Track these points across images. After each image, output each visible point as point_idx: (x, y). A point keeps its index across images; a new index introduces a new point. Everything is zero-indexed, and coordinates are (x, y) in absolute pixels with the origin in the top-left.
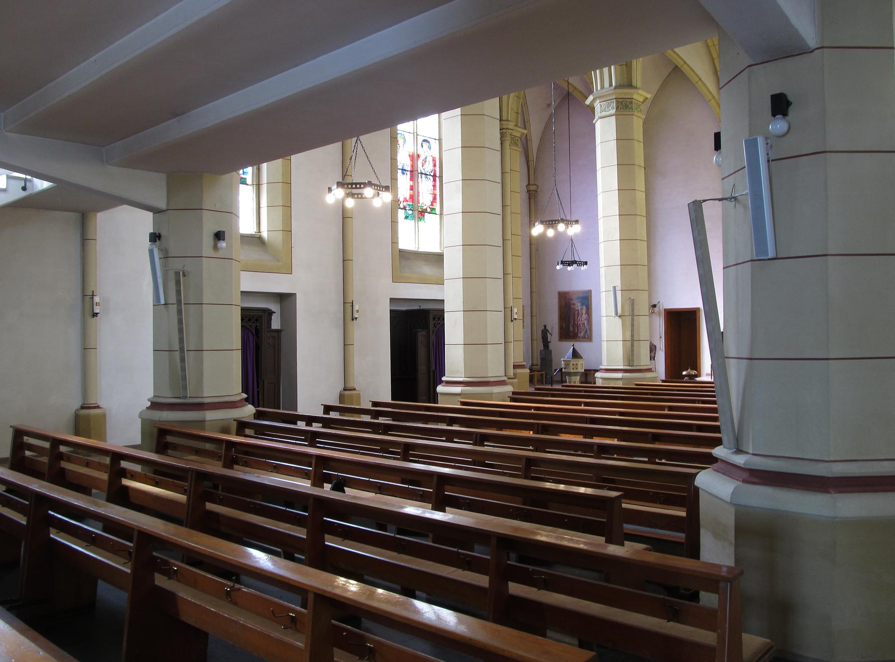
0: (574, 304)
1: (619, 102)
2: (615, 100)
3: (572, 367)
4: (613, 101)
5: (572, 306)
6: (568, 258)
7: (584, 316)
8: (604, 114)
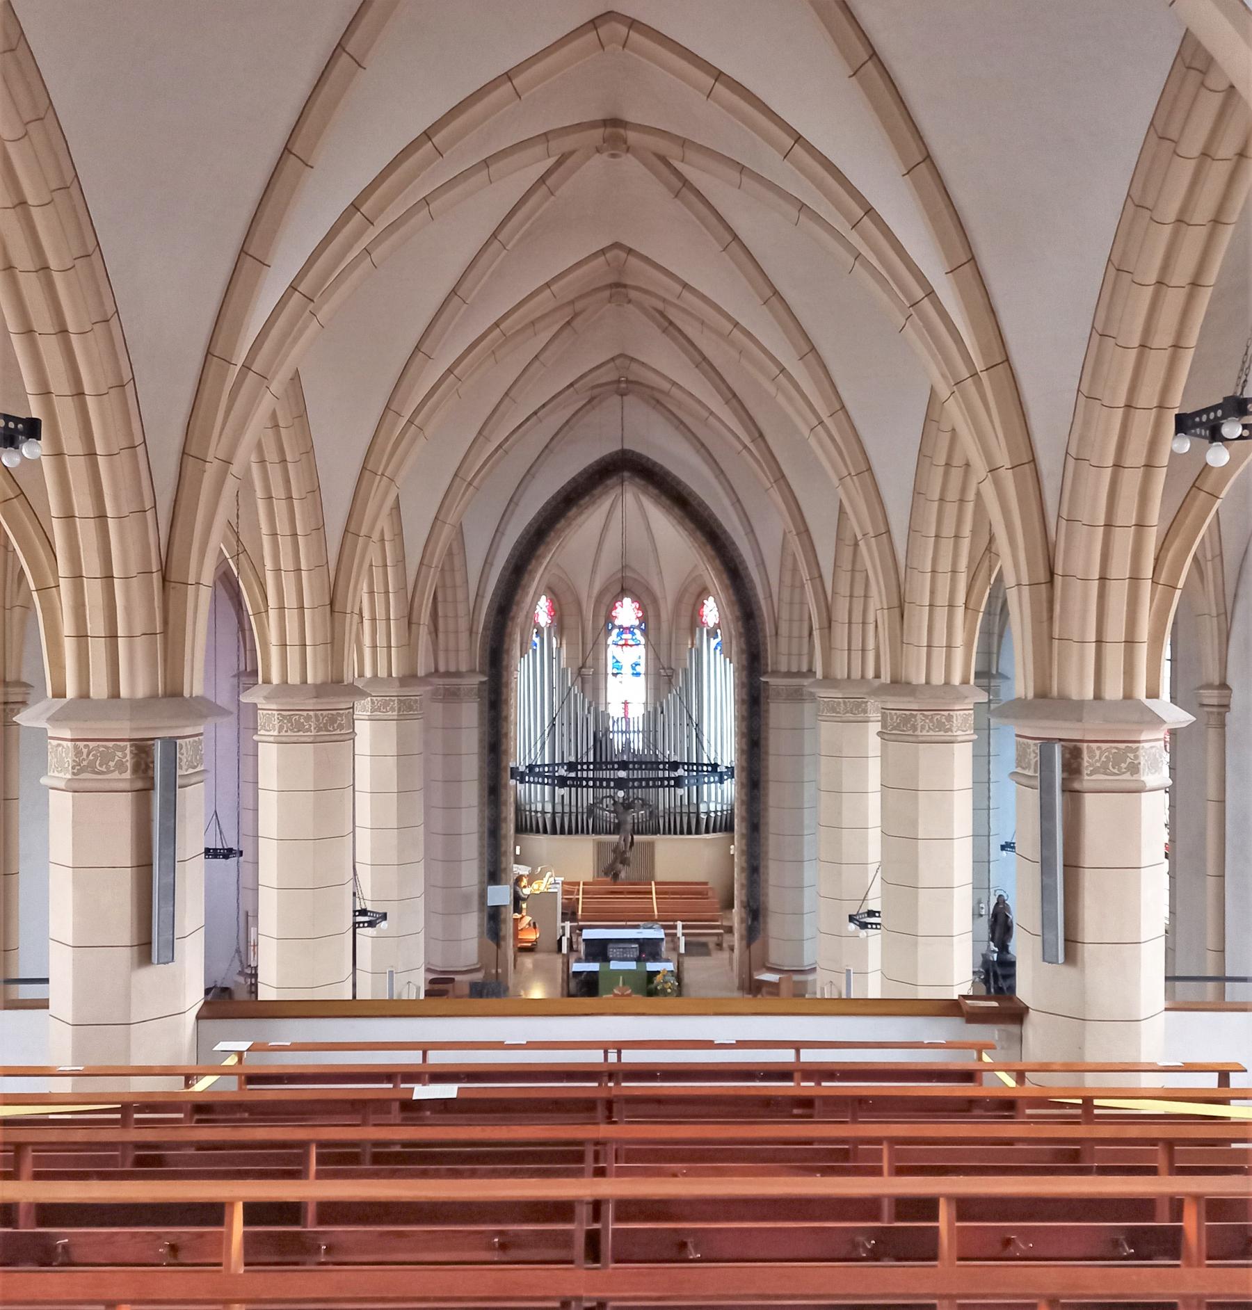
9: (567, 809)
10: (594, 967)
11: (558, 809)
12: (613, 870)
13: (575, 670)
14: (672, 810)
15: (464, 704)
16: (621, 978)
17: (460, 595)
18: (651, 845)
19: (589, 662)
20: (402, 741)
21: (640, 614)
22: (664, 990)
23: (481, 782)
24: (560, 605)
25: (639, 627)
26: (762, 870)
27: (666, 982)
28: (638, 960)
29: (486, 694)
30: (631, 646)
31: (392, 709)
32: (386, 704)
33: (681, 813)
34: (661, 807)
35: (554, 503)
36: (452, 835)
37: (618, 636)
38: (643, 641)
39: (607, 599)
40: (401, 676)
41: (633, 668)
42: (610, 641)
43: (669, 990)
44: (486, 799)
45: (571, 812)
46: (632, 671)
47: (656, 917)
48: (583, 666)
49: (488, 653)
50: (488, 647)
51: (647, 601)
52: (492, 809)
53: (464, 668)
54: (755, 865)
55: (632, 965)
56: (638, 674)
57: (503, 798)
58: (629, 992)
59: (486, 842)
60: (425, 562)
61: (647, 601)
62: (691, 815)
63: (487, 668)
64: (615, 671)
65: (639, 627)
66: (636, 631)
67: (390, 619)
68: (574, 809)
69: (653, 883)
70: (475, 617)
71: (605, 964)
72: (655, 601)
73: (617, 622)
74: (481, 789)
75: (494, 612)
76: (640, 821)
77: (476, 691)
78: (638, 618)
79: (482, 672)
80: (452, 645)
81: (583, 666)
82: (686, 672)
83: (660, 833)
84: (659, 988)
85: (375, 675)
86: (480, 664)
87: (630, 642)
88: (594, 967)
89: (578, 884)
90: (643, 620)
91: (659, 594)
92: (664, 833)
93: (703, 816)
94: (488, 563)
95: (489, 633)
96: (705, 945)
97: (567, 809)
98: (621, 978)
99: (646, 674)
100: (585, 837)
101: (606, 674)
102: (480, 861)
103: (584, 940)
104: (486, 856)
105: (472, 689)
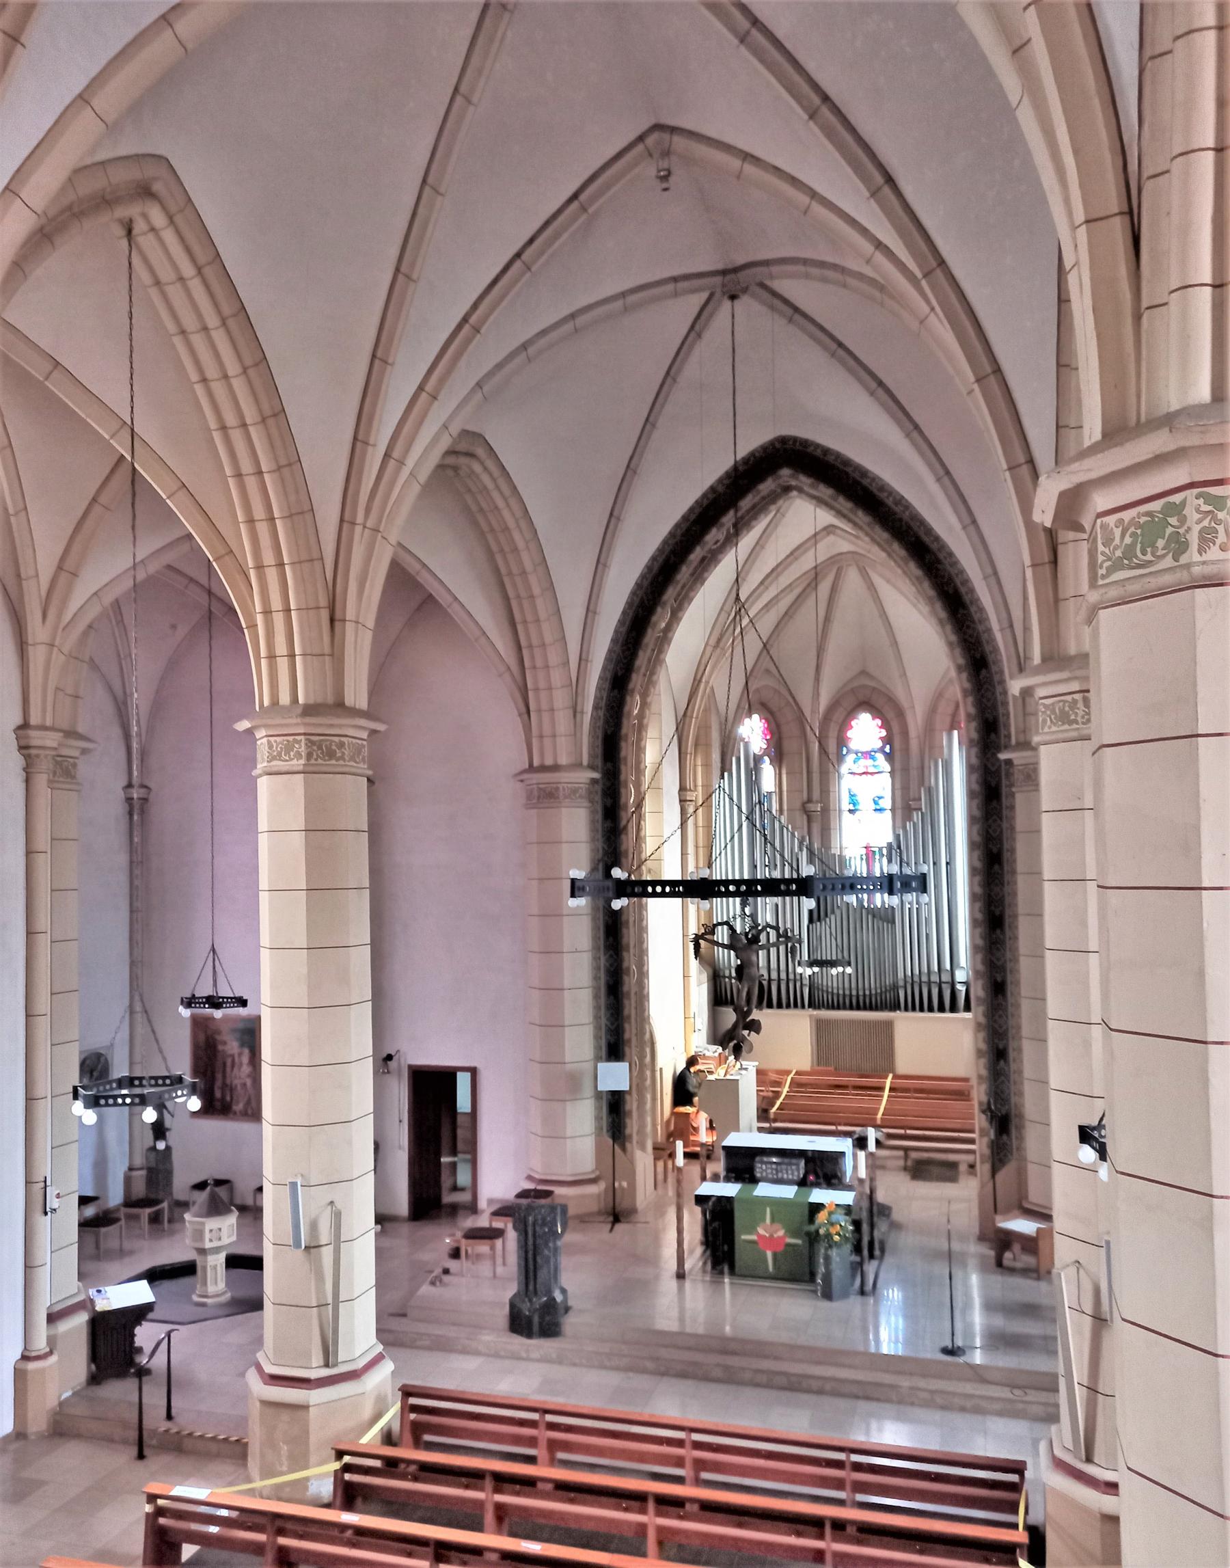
0: (225, 1043)
1: (313, 743)
2: (302, 737)
3: (207, 1236)
4: (298, 738)
5: (220, 1047)
6: (205, 990)
7: (246, 1069)
8: (278, 765)
10: (730, 1189)
12: (731, 1039)
13: (798, 804)
14: (916, 979)
15: (564, 810)
16: (768, 1210)
17: (554, 658)
18: (889, 1025)
19: (816, 794)
20: (313, 805)
21: (884, 733)
22: (828, 1236)
23: (594, 919)
24: (778, 726)
25: (882, 750)
26: (1012, 1054)
27: (832, 1224)
28: (802, 1183)
29: (598, 798)
30: (872, 774)
31: (299, 755)
32: (288, 748)
34: (901, 975)
35: (684, 526)
36: (552, 990)
37: (855, 762)
38: (888, 768)
39: (839, 715)
40: (311, 702)
41: (876, 803)
42: (844, 769)
43: (837, 1238)
44: (602, 942)
45: (779, 980)
46: (874, 807)
47: (879, 1122)
48: (809, 801)
49: (599, 742)
50: (600, 734)
51: (890, 715)
52: (611, 956)
53: (563, 760)
54: (1001, 1047)
55: (789, 1192)
56: (880, 810)
57: (624, 941)
58: (781, 1233)
59: (603, 1001)
60: (347, 517)
61: (890, 715)
63: (599, 762)
64: (852, 807)
65: (882, 750)
66: (880, 757)
67: (290, 610)
68: (783, 976)
69: (891, 1076)
70: (579, 691)
71: (749, 1186)
72: (900, 714)
73: (853, 745)
74: (595, 928)
75: (607, 685)
76: (873, 992)
77: (583, 792)
78: (881, 738)
79: (592, 767)
80: (547, 730)
81: (809, 801)
82: (930, 792)
83: (899, 1009)
84: (822, 1231)
85: (275, 702)
86: (590, 756)
87: (871, 770)
88: (730, 1189)
89: (788, 1072)
90: (888, 740)
91: (904, 703)
92: (906, 1009)
93: (959, 987)
94: (591, 611)
95: (601, 713)
96: (953, 1166)
98: (768, 1210)
99: (893, 810)
100: (792, 1012)
101: (840, 810)
102: (595, 1028)
103: (724, 1148)
104: (604, 1021)
105: (574, 791)
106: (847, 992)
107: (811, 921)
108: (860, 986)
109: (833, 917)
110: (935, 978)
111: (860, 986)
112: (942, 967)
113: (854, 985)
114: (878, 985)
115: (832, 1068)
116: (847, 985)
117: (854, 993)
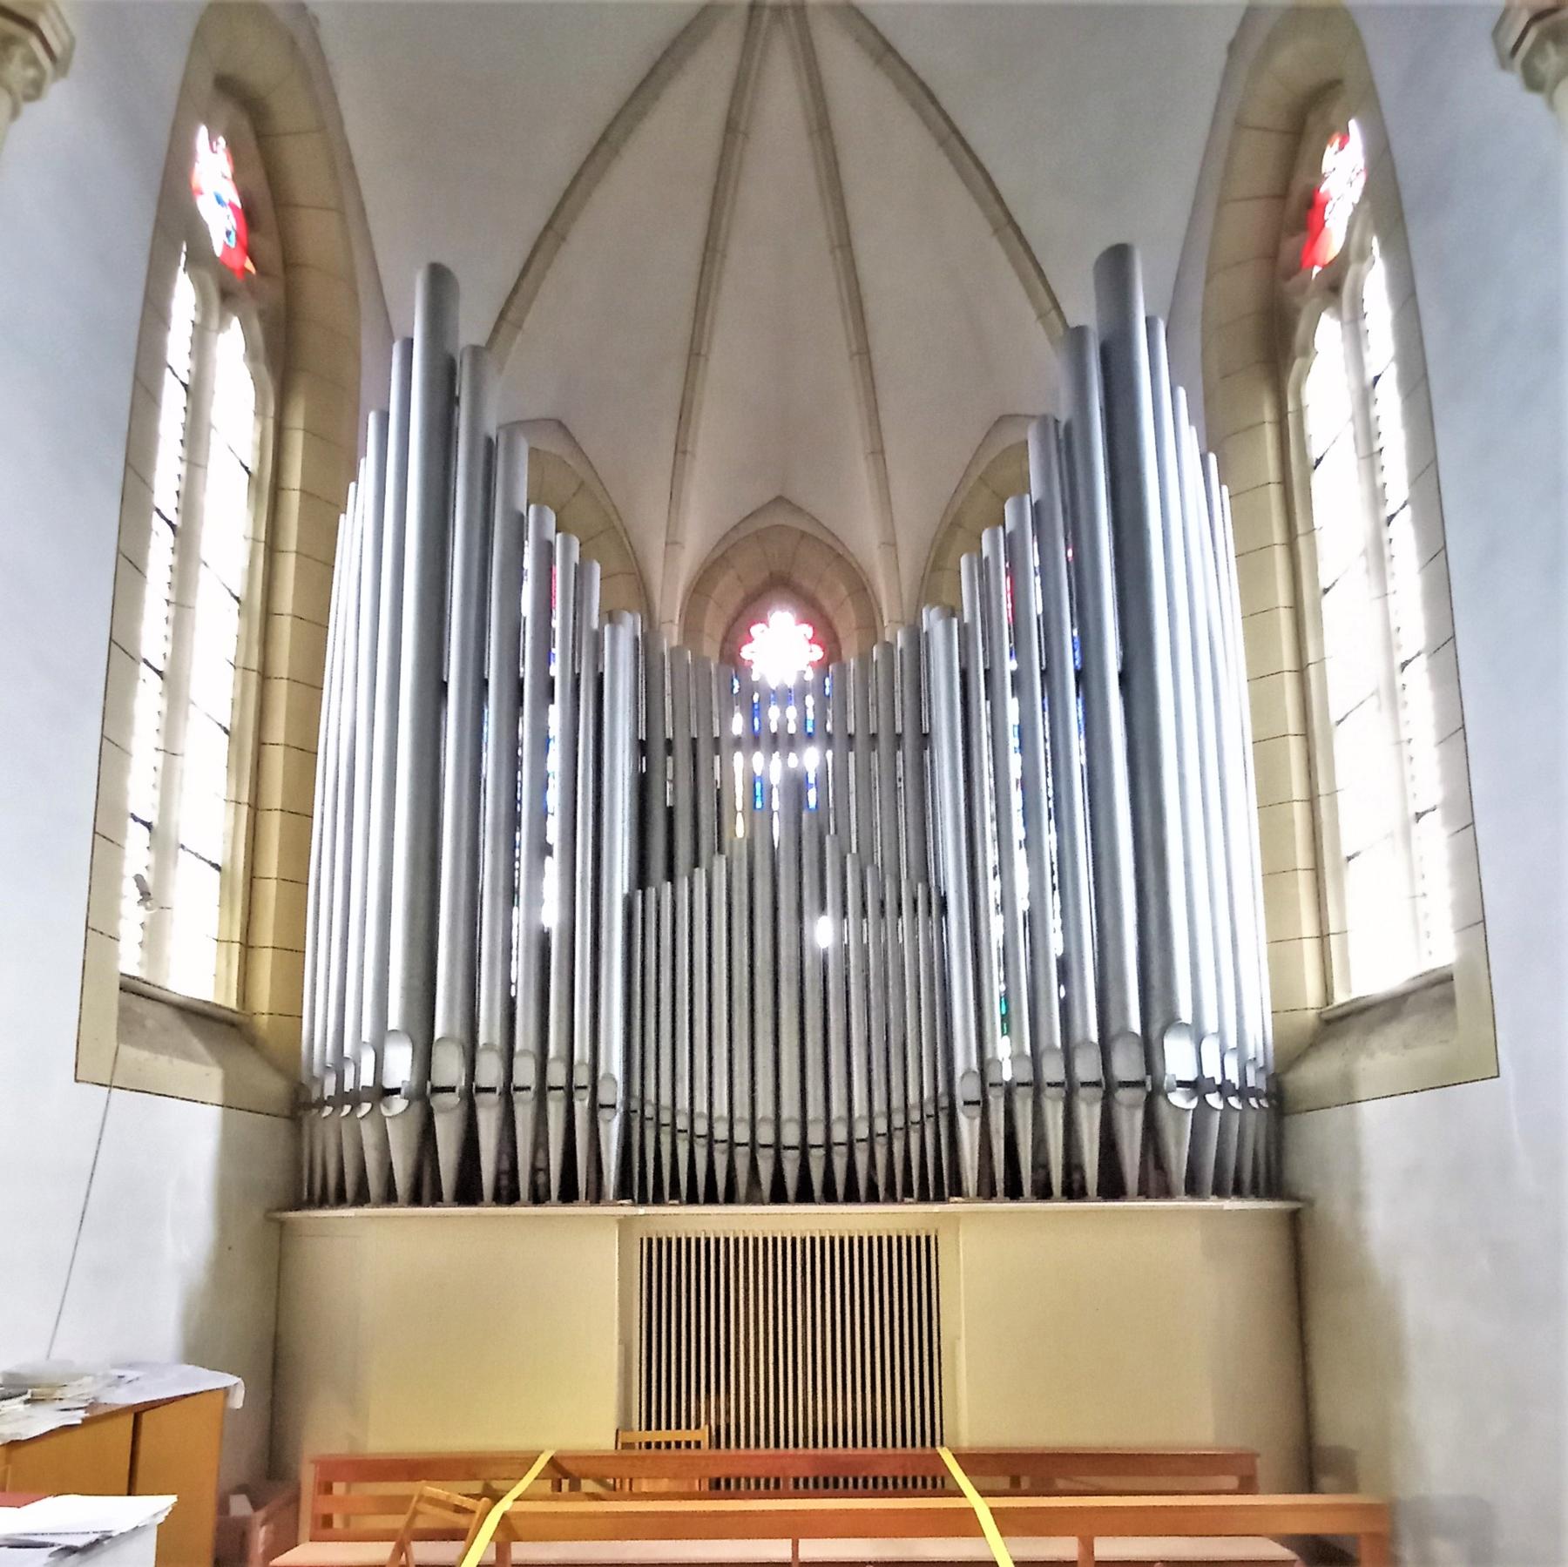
9: (490, 1071)
11: (449, 1068)
33: (1070, 1088)
34: (964, 1059)
45: (508, 1092)
62: (1123, 1095)
68: (525, 1072)
76: (862, 1131)
92: (987, 1191)
93: (1178, 1098)
97: (490, 1071)
106: (765, 1135)
107: (641, 878)
108: (815, 1110)
109: (720, 865)
110: (1087, 1067)
111: (815, 1110)
112: (1114, 1028)
113: (790, 1109)
114: (880, 1105)
115: (702, 1435)
116: (765, 1108)
117: (791, 1135)
